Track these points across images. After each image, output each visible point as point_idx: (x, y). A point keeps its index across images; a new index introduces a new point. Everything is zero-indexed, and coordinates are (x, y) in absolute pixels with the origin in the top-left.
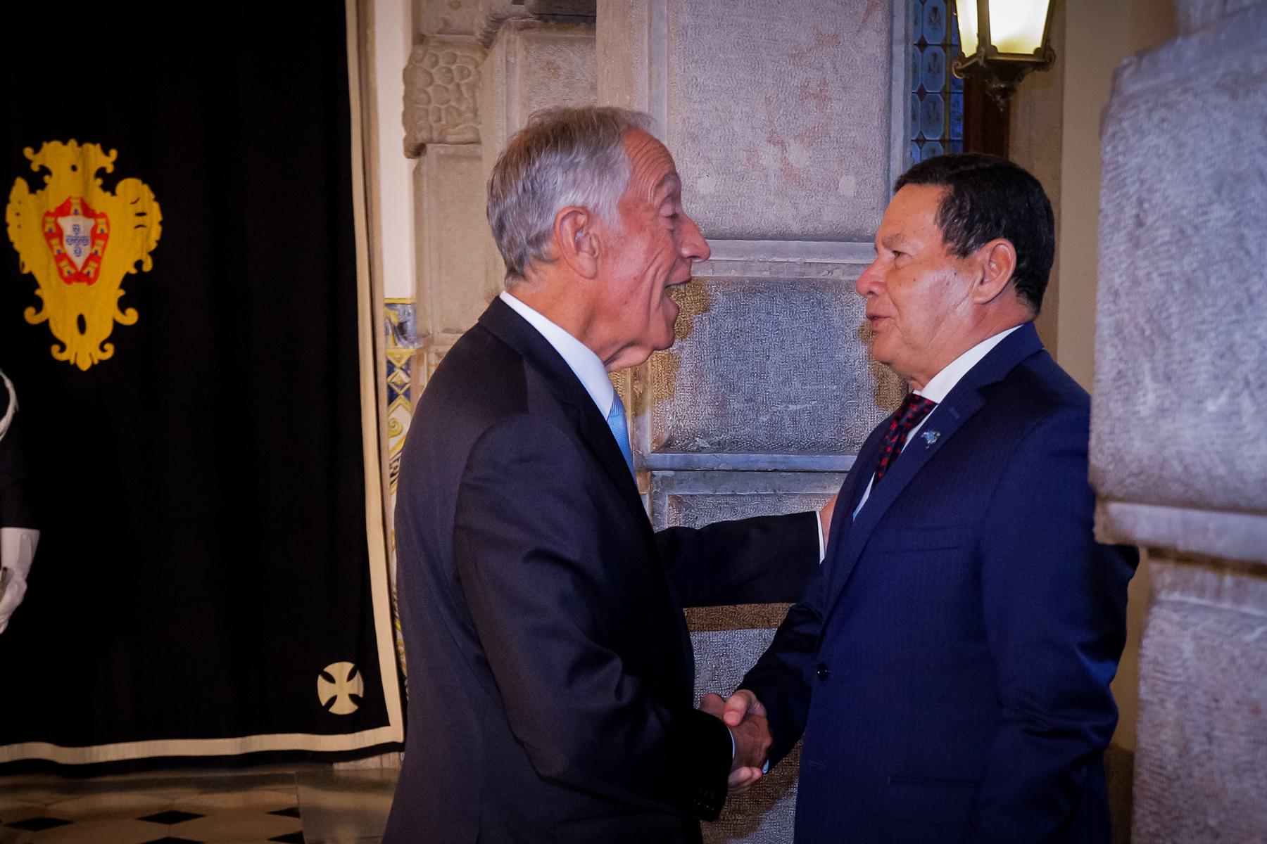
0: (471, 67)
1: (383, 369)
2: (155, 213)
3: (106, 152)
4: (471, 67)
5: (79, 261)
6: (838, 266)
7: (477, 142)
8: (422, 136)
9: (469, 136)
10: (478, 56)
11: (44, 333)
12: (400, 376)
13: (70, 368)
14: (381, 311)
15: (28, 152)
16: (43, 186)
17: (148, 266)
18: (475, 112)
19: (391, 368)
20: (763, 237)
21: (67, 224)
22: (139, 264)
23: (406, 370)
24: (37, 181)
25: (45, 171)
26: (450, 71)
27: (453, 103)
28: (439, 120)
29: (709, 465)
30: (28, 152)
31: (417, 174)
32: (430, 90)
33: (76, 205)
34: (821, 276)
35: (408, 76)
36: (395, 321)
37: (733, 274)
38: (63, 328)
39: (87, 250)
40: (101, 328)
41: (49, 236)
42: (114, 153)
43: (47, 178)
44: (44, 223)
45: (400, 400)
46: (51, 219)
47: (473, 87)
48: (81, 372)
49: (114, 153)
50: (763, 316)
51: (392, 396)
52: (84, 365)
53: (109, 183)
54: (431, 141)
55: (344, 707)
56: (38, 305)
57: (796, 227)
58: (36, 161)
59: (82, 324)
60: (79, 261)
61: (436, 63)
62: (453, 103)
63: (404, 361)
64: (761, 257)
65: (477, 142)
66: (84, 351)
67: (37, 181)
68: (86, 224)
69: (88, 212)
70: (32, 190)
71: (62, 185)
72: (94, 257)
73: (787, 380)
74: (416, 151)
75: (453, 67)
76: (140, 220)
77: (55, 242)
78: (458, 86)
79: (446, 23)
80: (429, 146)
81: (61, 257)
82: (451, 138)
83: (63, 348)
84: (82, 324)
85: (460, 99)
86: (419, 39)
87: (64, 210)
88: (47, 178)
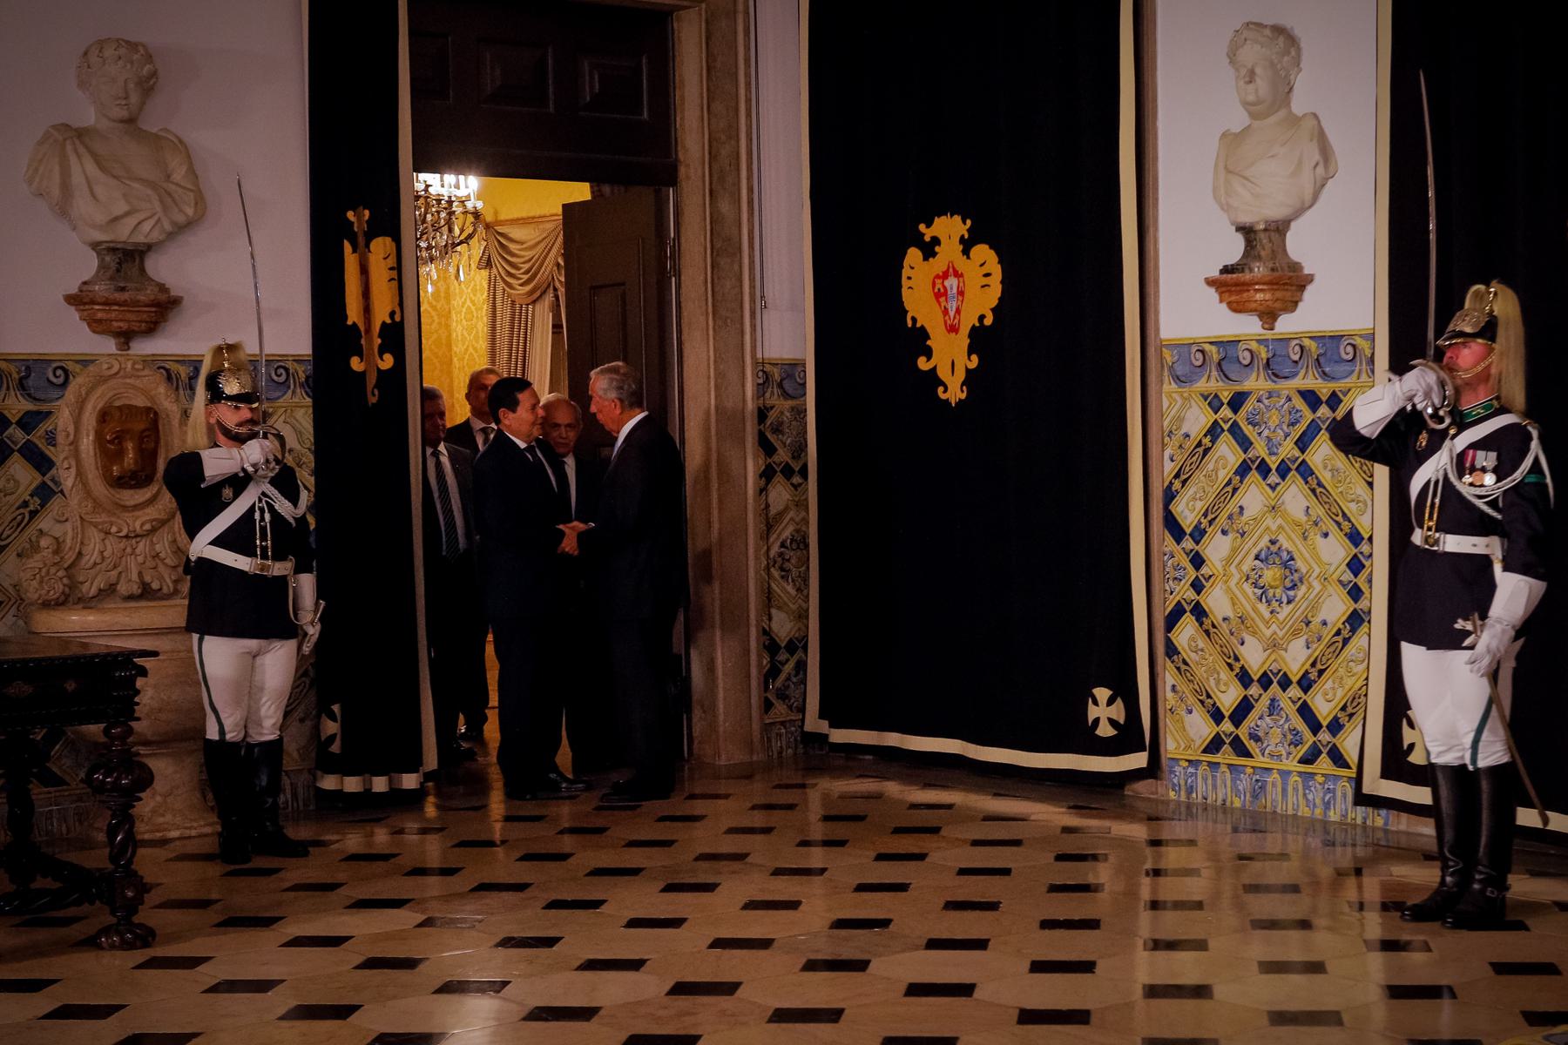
11: (932, 378)
15: (922, 227)
16: (934, 254)
17: (988, 321)
24: (929, 249)
25: (936, 241)
30: (922, 227)
38: (943, 373)
41: (938, 295)
43: (937, 249)
44: (934, 285)
46: (939, 281)
55: (1105, 731)
56: (929, 353)
58: (928, 233)
67: (929, 249)
70: (926, 259)
71: (949, 251)
76: (985, 281)
77: (942, 299)
88: (937, 249)
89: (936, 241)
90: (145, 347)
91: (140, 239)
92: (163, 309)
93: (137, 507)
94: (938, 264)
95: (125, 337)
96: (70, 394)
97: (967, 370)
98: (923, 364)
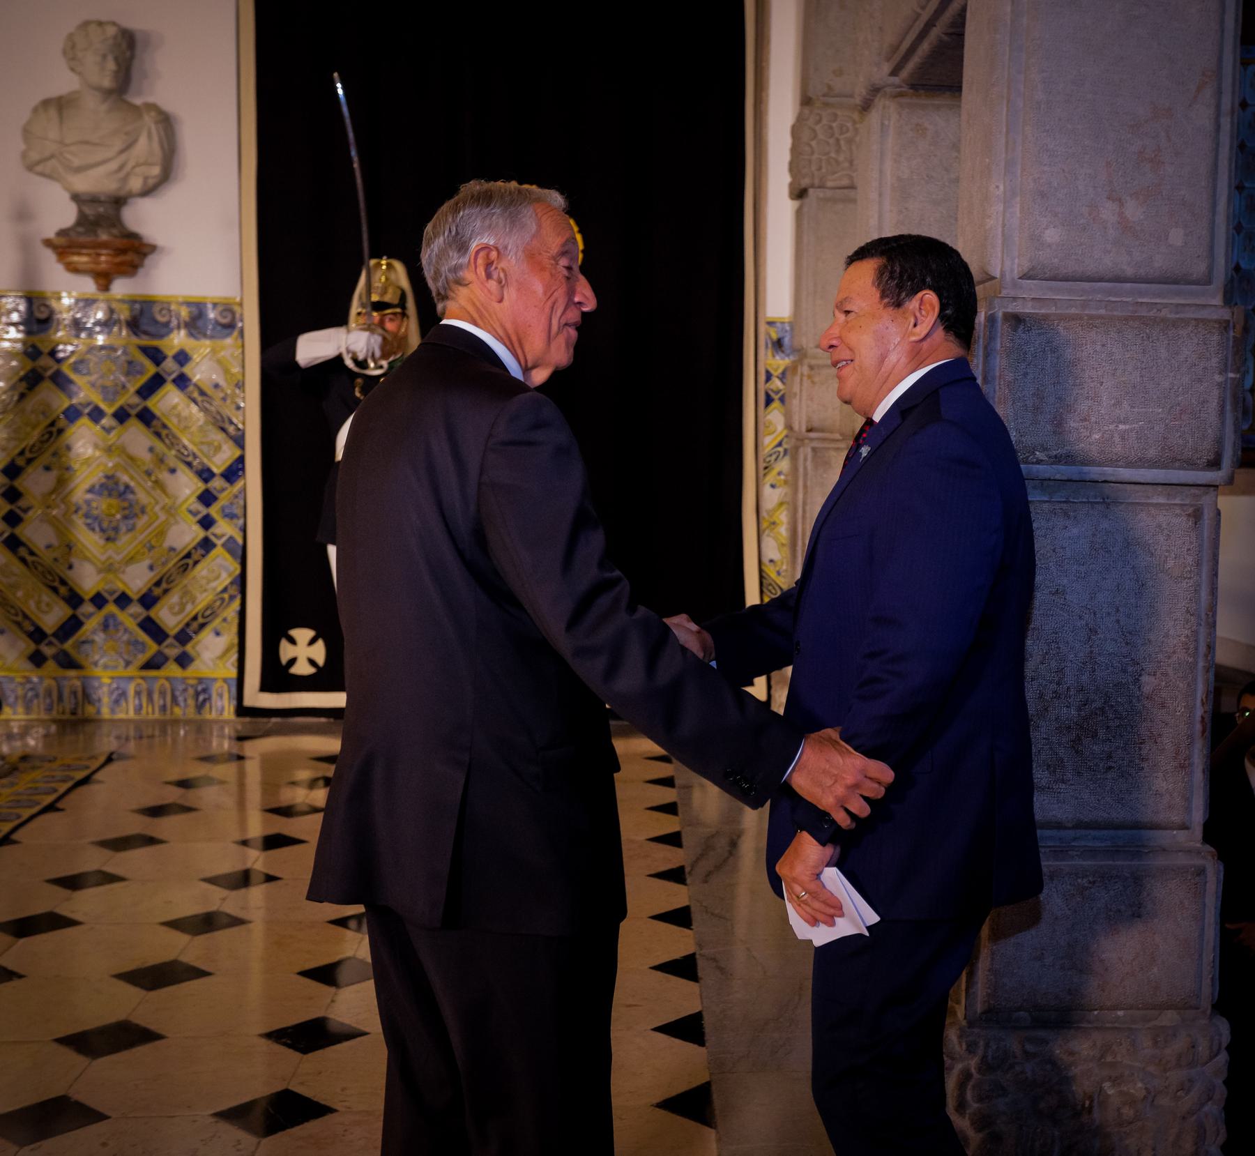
0: (849, 125)
1: (762, 377)
4: (849, 125)
6: (1166, 306)
7: (852, 187)
8: (805, 182)
9: (845, 182)
10: (856, 116)
12: (777, 384)
14: (763, 328)
18: (851, 163)
19: (769, 377)
20: (1101, 280)
23: (782, 377)
26: (831, 128)
27: (833, 155)
28: (820, 169)
29: (1047, 476)
31: (799, 214)
32: (814, 143)
34: (1151, 314)
35: (796, 131)
36: (774, 336)
37: (1073, 311)
45: (776, 404)
47: (850, 141)
48: (296, 364)
50: (1098, 348)
51: (769, 401)
54: (812, 186)
57: (1129, 271)
61: (819, 121)
62: (833, 155)
63: (780, 371)
64: (1099, 297)
65: (852, 187)
73: (1118, 403)
74: (799, 193)
75: (834, 125)
78: (838, 140)
79: (830, 87)
80: (811, 191)
82: (830, 184)
85: (838, 151)
86: (806, 101)
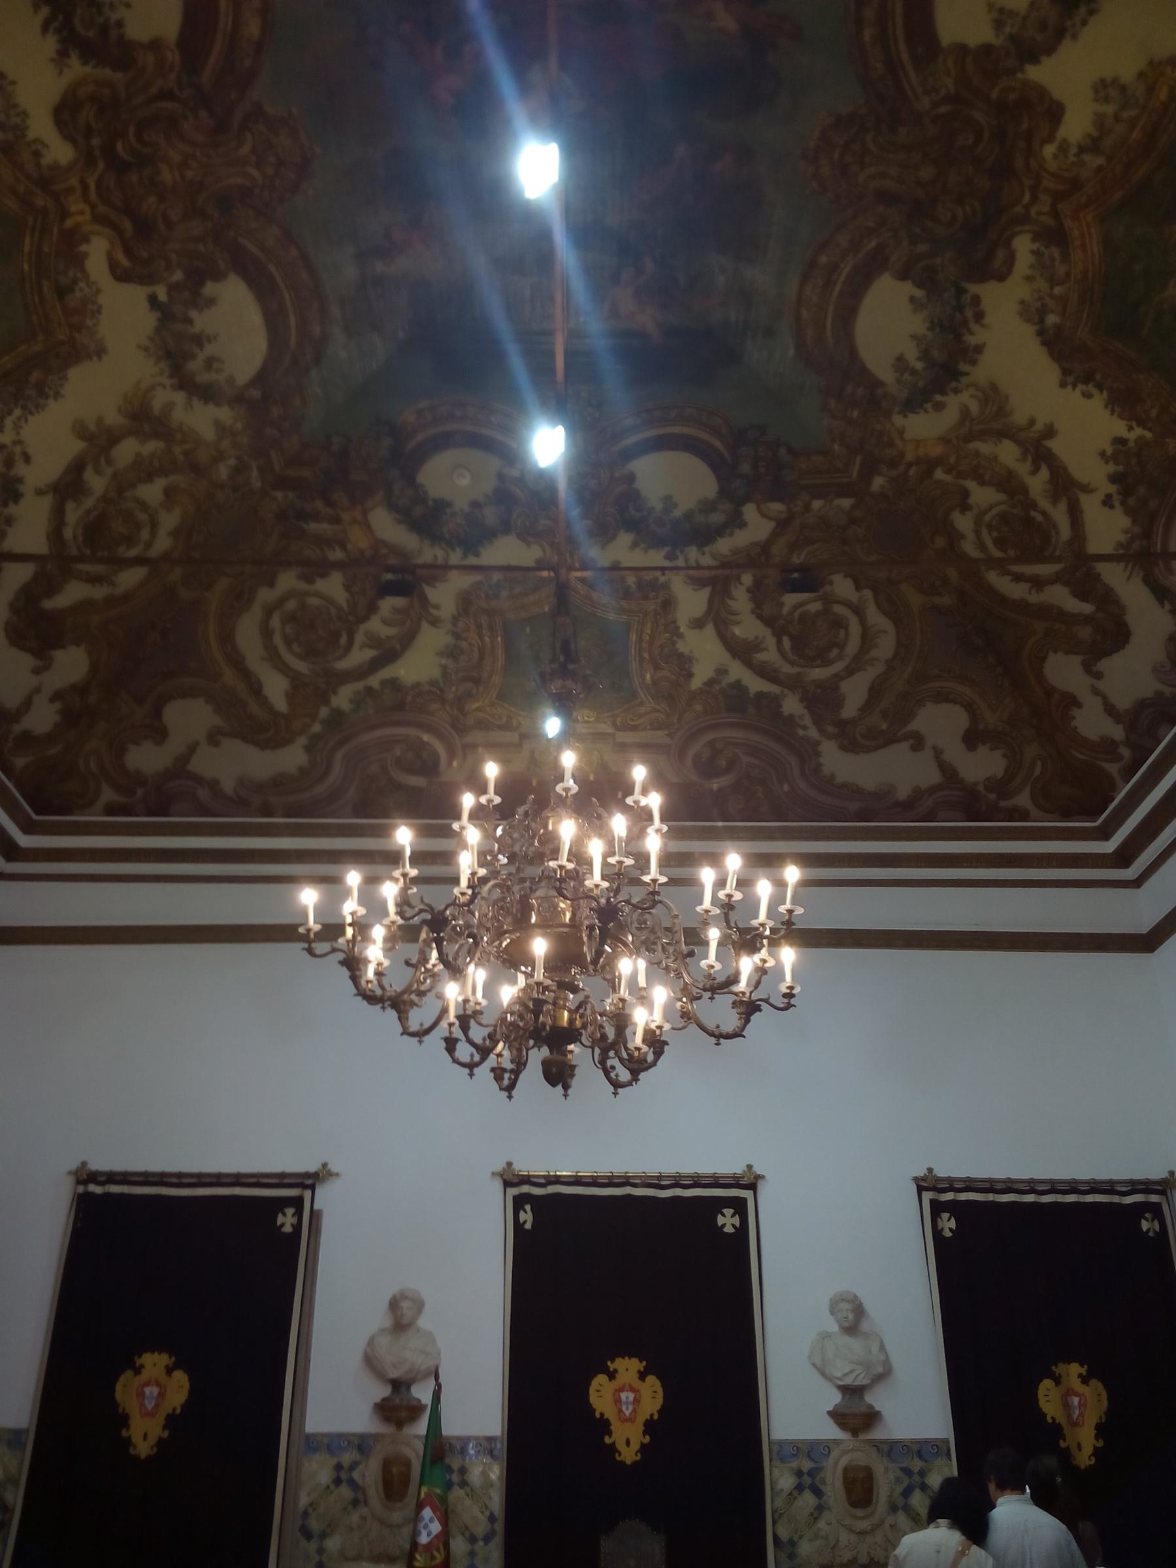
2: (661, 1393)
3: (641, 1361)
5: (627, 1413)
11: (613, 1448)
13: (623, 1463)
15: (609, 1363)
17: (656, 1417)
21: (623, 1396)
22: (652, 1415)
25: (615, 1371)
30: (609, 1363)
33: (627, 1387)
38: (620, 1446)
39: (631, 1408)
40: (635, 1446)
42: (644, 1363)
49: (644, 1363)
52: (629, 1462)
53: (642, 1376)
56: (610, 1434)
58: (611, 1366)
59: (628, 1443)
60: (627, 1413)
66: (629, 1455)
67: (612, 1376)
68: (631, 1396)
69: (632, 1390)
72: (634, 1411)
81: (620, 1411)
83: (620, 1455)
84: (628, 1443)
87: (622, 1389)
89: (615, 1371)
90: (863, 1437)
91: (857, 1383)
92: (871, 1418)
93: (860, 1518)
94: (616, 1384)
95: (855, 1432)
96: (831, 1460)
97: (642, 1444)
98: (607, 1440)
